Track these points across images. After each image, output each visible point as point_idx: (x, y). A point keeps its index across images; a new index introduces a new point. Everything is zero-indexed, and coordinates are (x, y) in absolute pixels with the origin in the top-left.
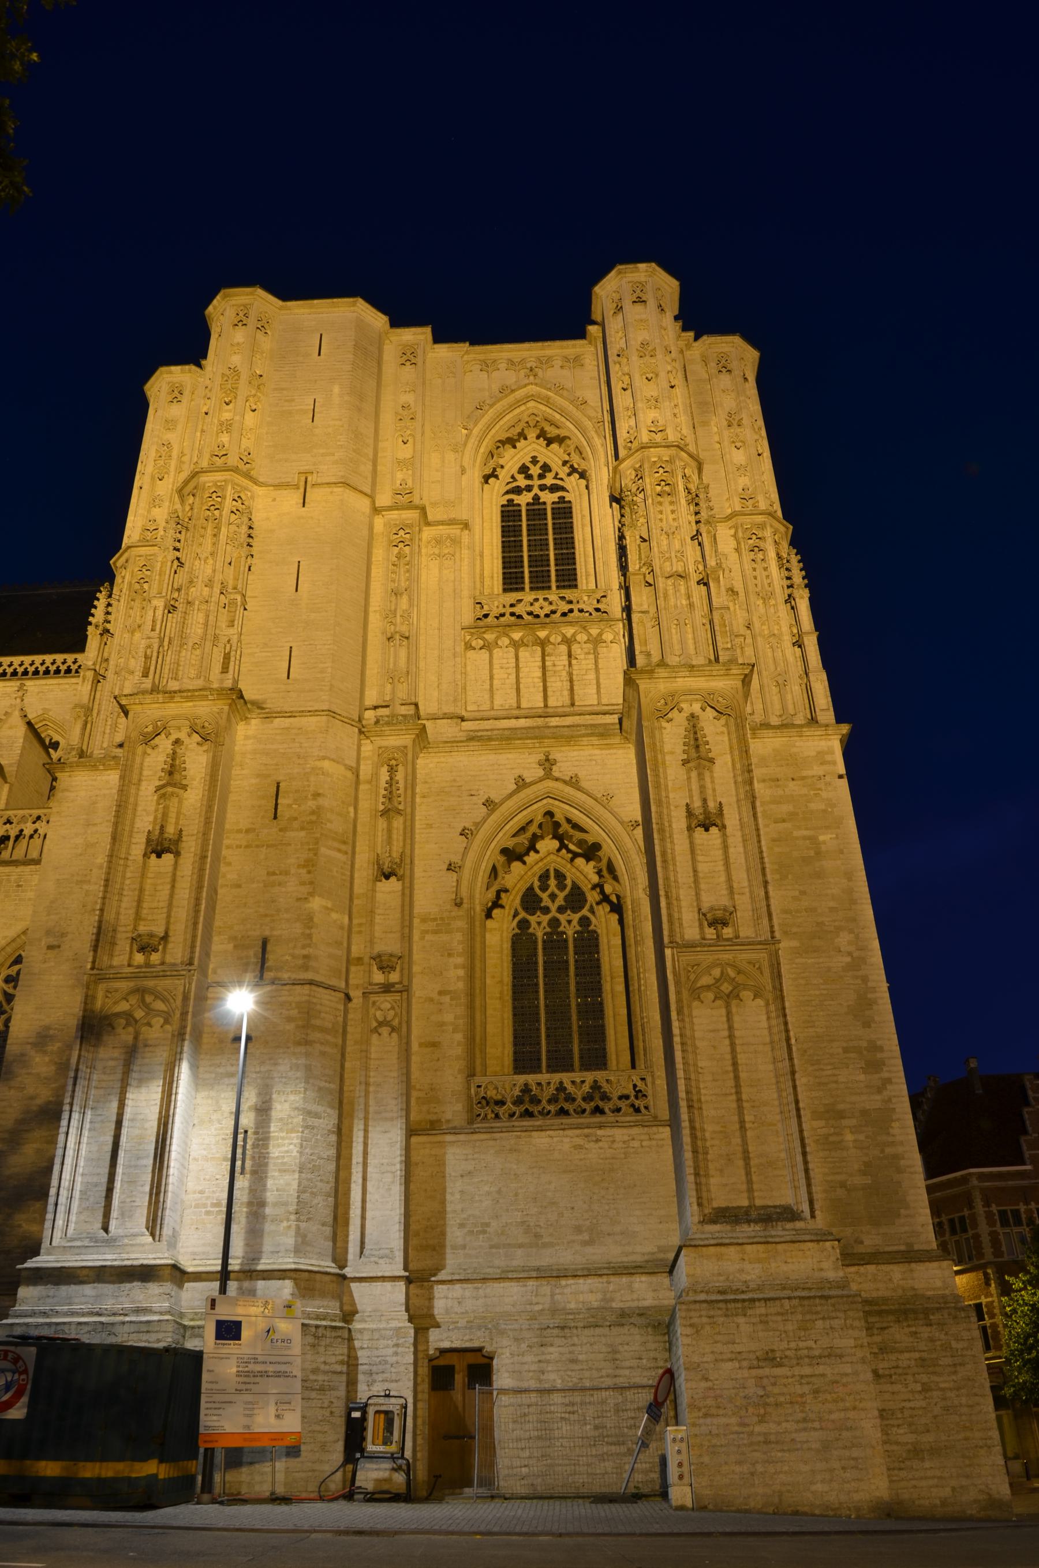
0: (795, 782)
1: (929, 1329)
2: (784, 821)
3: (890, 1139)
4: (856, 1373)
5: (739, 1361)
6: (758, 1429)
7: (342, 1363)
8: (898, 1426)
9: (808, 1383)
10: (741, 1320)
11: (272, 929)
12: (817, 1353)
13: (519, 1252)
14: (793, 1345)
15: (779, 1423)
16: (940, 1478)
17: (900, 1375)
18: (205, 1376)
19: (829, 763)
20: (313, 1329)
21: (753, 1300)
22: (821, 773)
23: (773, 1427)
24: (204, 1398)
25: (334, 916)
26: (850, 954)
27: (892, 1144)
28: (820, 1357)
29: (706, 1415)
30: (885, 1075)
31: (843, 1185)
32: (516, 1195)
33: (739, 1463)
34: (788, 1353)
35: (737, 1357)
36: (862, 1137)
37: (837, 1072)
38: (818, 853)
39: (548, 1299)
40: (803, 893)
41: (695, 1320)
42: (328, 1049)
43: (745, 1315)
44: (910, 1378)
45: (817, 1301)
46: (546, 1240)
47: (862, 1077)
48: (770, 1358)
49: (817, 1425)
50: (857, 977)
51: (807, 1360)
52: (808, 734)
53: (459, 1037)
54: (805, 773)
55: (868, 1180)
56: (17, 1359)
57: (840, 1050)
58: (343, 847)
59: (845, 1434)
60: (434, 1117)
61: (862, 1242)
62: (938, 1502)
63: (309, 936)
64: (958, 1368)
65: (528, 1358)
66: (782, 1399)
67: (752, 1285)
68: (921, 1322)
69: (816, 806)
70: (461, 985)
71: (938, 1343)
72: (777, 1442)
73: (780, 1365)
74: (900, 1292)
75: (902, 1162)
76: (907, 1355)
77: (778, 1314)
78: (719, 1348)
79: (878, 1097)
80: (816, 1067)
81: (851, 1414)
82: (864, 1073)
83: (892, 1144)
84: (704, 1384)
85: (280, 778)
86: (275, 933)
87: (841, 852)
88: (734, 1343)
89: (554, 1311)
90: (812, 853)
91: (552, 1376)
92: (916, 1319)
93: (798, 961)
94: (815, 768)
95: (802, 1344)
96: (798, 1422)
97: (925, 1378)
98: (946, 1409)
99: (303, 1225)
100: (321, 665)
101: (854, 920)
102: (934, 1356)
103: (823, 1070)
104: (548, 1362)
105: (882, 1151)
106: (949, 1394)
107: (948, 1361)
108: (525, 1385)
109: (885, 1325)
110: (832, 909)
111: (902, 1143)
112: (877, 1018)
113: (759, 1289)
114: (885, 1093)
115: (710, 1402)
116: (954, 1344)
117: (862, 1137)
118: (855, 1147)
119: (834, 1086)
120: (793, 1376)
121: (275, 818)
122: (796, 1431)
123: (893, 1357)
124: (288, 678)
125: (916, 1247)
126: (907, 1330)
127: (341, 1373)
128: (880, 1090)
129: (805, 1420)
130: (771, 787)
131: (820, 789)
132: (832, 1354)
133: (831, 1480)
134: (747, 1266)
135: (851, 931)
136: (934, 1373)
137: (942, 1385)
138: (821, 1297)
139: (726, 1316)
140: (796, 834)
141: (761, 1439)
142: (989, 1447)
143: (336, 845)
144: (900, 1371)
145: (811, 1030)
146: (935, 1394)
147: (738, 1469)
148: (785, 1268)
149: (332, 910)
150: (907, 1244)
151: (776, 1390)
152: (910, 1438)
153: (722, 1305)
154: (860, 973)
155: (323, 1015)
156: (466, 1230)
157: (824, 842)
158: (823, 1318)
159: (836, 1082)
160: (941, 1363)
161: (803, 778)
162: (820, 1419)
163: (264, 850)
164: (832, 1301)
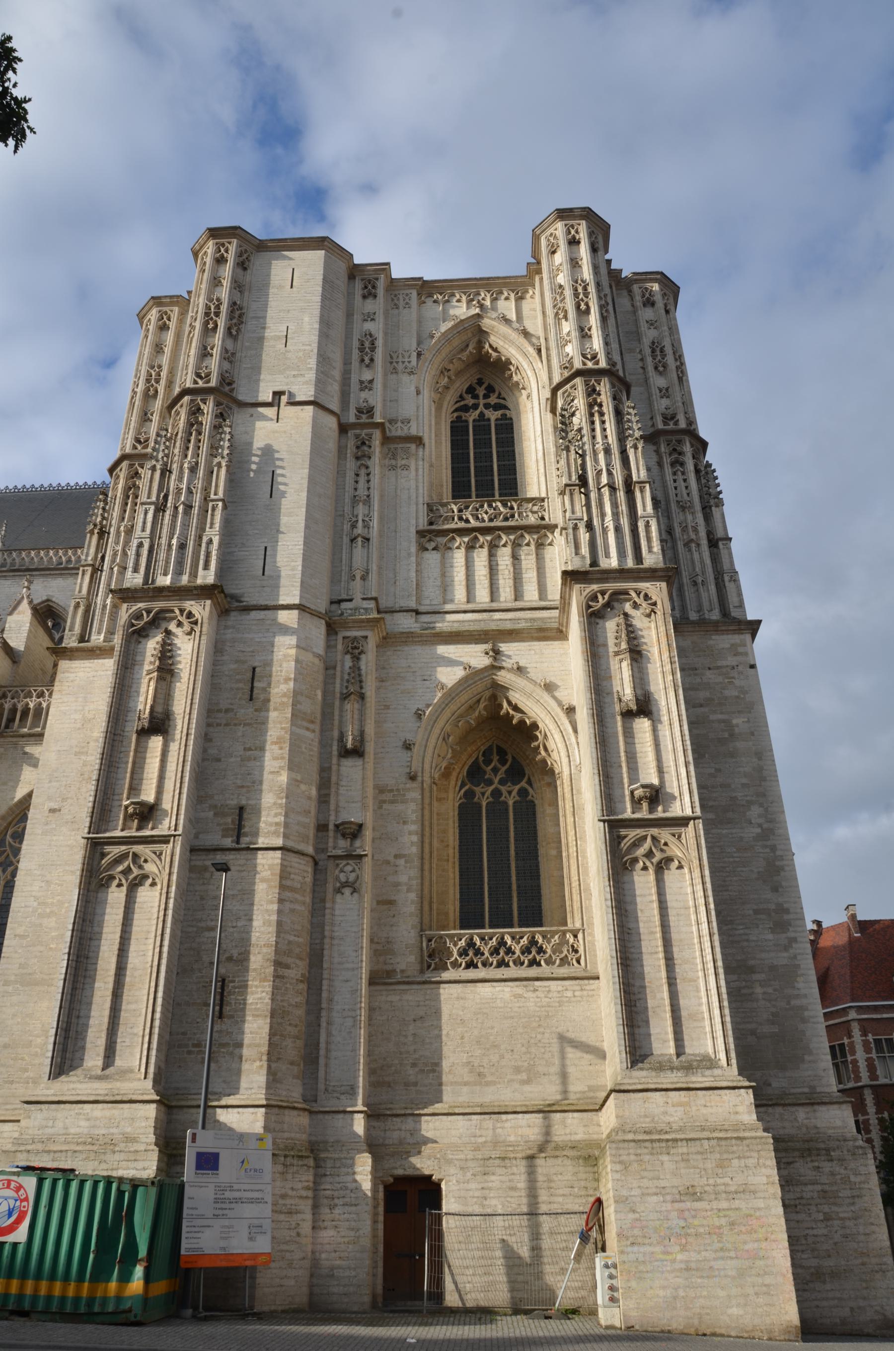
1: (830, 1164)
2: (701, 706)
3: (796, 992)
4: (768, 1208)
5: (663, 1195)
6: (680, 1257)
7: (307, 1188)
8: (803, 1251)
9: (725, 1216)
10: (665, 1158)
11: (248, 799)
12: (733, 1189)
13: (465, 1089)
14: (711, 1181)
15: (699, 1252)
16: (840, 1299)
17: (804, 1205)
18: (187, 1203)
19: (741, 654)
20: (282, 1159)
21: (675, 1140)
22: (734, 663)
23: (694, 1256)
24: (185, 1223)
25: (303, 787)
26: (760, 826)
27: (798, 996)
28: (736, 1193)
29: (633, 1244)
30: (792, 935)
31: (753, 1033)
32: (462, 1038)
33: (664, 1288)
34: (707, 1188)
35: (661, 1191)
36: (770, 990)
37: (747, 931)
38: (732, 735)
39: (490, 1132)
41: (624, 1158)
42: (297, 907)
43: (668, 1154)
44: (813, 1208)
45: (734, 1141)
46: (489, 1079)
47: (770, 936)
48: (691, 1193)
49: (732, 1254)
50: (766, 847)
51: (724, 1195)
52: (723, 628)
53: (413, 896)
54: (720, 663)
56: (19, 1188)
57: (751, 912)
58: (311, 726)
59: (760, 1263)
60: (389, 968)
61: (770, 1085)
62: (838, 1321)
64: (856, 1200)
65: (473, 1186)
66: (701, 1230)
67: (675, 1126)
68: (823, 1158)
69: (731, 692)
70: (414, 850)
71: (838, 1177)
72: (697, 1270)
73: (700, 1199)
74: (804, 1130)
75: (806, 1013)
76: (810, 1187)
77: (698, 1153)
78: (645, 1183)
79: (785, 954)
80: (730, 927)
81: (764, 1245)
82: (772, 932)
83: (798, 996)
84: (631, 1216)
85: (256, 664)
86: (250, 802)
87: (752, 734)
88: (658, 1179)
89: (496, 1143)
90: (726, 735)
91: (494, 1202)
92: (818, 1155)
93: (713, 831)
94: (729, 658)
95: (719, 1181)
96: (716, 1251)
97: (826, 1209)
98: (845, 1236)
99: (273, 1065)
100: (293, 564)
101: (764, 795)
102: (835, 1188)
103: (736, 929)
104: (490, 1189)
105: (788, 1003)
106: (848, 1223)
107: (848, 1193)
108: (470, 1210)
109: (791, 1160)
110: (744, 785)
111: (805, 996)
112: (784, 884)
113: (681, 1130)
114: (791, 951)
115: (636, 1232)
116: (853, 1178)
117: (770, 990)
118: (764, 999)
119: (745, 944)
120: (712, 1210)
121: (251, 699)
122: (715, 1259)
123: (798, 1189)
124: (263, 574)
125: (818, 1090)
126: (810, 1165)
127: (307, 1197)
128: (786, 948)
129: (722, 1249)
130: (690, 675)
131: (734, 678)
132: (746, 1190)
133: (746, 1305)
134: (671, 1110)
135: (761, 805)
136: (835, 1204)
137: (841, 1215)
138: (738, 1138)
139: (652, 1154)
140: (713, 717)
141: (683, 1266)
142: (884, 1272)
143: (305, 724)
144: (804, 1201)
145: (725, 893)
146: (836, 1223)
147: (661, 1293)
148: (704, 1111)
149: (301, 782)
150: (810, 1087)
151: (696, 1222)
152: (814, 1262)
153: (648, 1144)
154: (769, 843)
155: (292, 876)
156: (417, 1069)
157: (737, 725)
158: (739, 1158)
159: (748, 940)
160: (841, 1195)
161: (718, 668)
162: (736, 1249)
163: (241, 728)
164: (745, 1142)
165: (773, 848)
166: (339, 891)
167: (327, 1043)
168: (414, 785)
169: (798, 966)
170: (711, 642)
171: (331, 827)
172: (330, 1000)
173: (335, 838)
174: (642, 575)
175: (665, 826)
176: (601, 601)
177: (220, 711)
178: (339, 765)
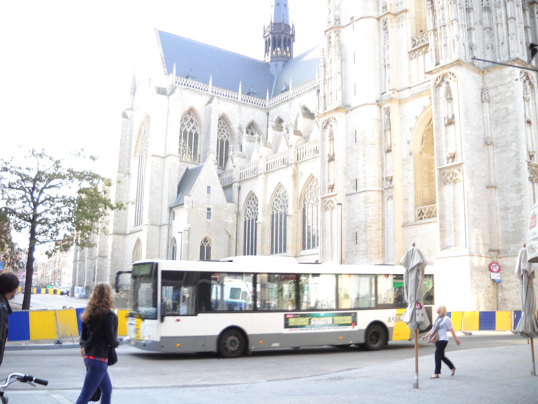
0: (502, 86)
2: (498, 103)
8: (509, 303)
22: (510, 80)
26: (515, 151)
31: (507, 232)
40: (502, 130)
44: (514, 290)
47: (515, 195)
53: (413, 196)
54: (506, 81)
55: (514, 230)
60: (407, 221)
63: (365, 177)
69: (509, 94)
83: (522, 217)
87: (515, 111)
90: (506, 114)
105: (519, 220)
110: (511, 135)
111: (524, 217)
117: (513, 216)
131: (510, 87)
135: (516, 142)
157: (510, 109)
161: (505, 84)
165: (519, 160)
166: (388, 199)
167: (387, 247)
168: (411, 157)
169: (523, 206)
170: (502, 73)
171: (385, 179)
172: (388, 234)
173: (386, 182)
174: (449, 66)
175: (456, 167)
176: (439, 80)
177: (349, 148)
178: (386, 156)
